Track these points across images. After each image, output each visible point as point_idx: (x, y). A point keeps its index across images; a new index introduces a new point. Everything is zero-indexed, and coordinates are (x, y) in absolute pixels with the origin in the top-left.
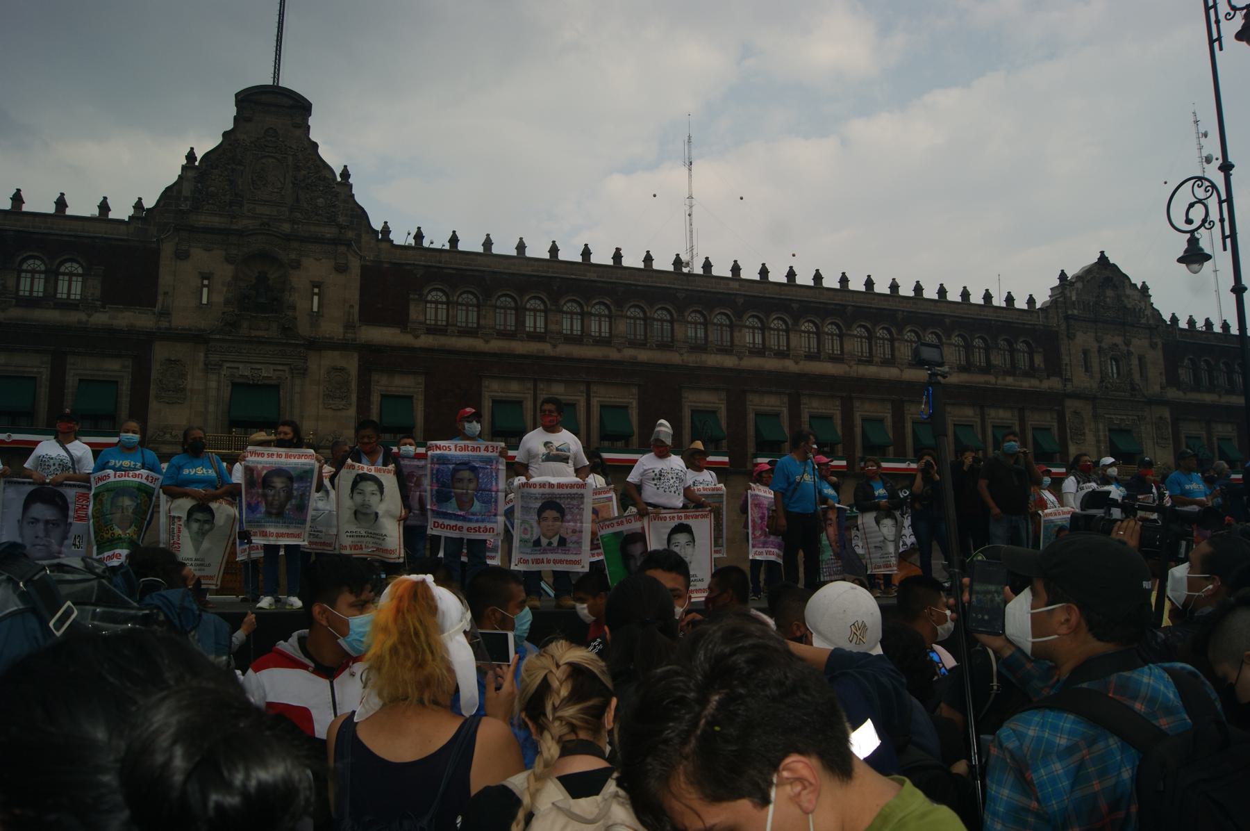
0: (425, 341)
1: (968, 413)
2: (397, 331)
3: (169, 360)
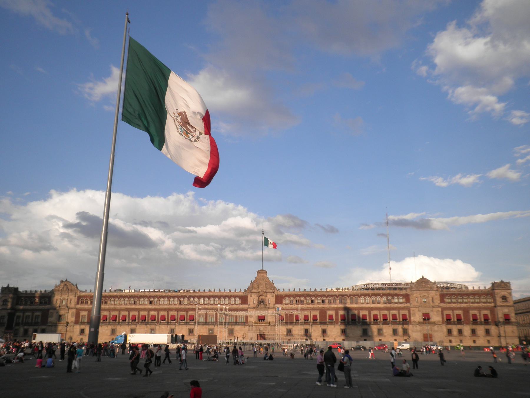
1: (386, 312)
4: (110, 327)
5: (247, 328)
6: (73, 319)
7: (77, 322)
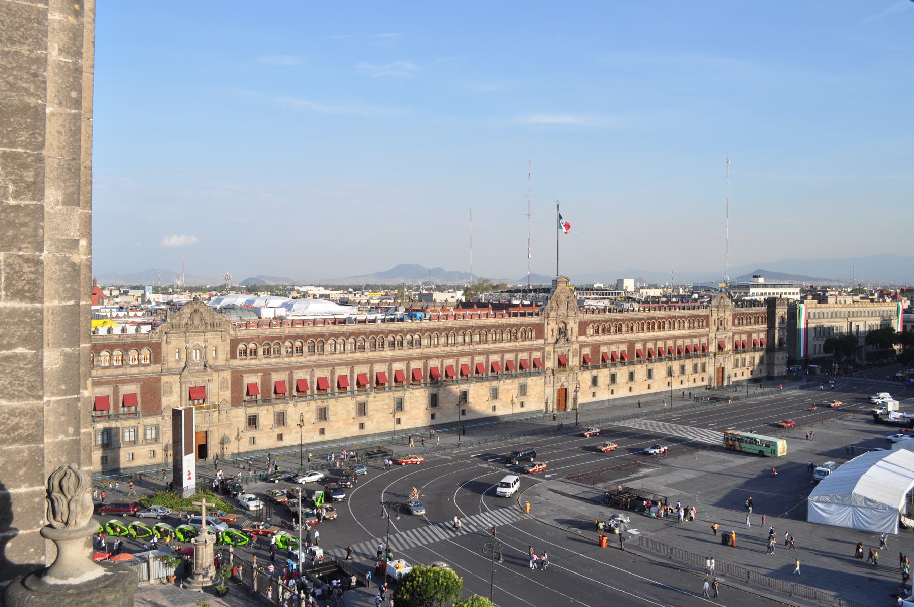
4: (313, 405)
6: (227, 395)
7: (236, 402)
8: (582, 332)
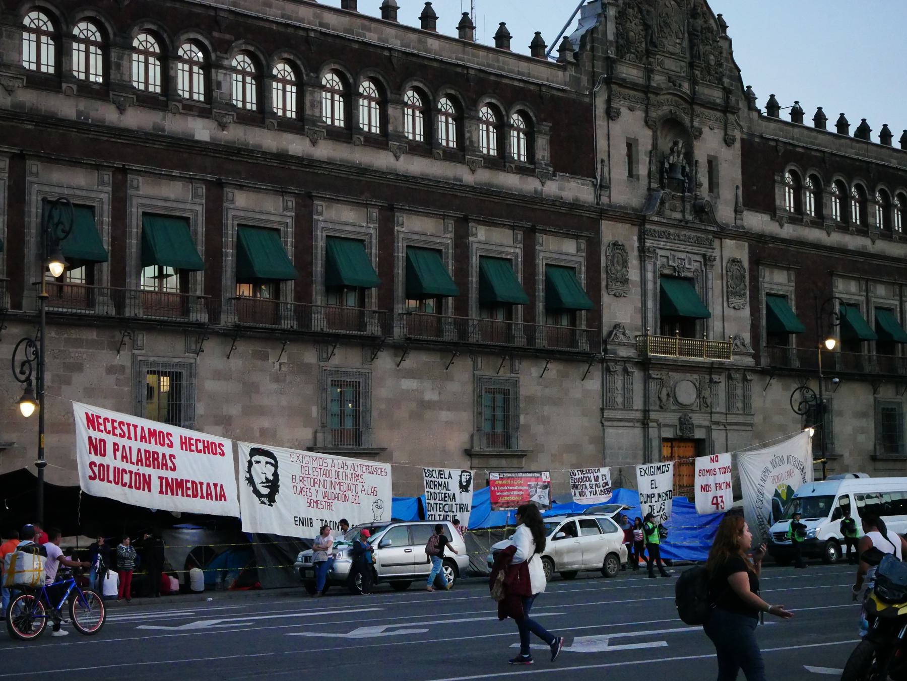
0: (788, 231)
2: (766, 218)
3: (615, 244)
5: (594, 384)
8: (757, 196)
